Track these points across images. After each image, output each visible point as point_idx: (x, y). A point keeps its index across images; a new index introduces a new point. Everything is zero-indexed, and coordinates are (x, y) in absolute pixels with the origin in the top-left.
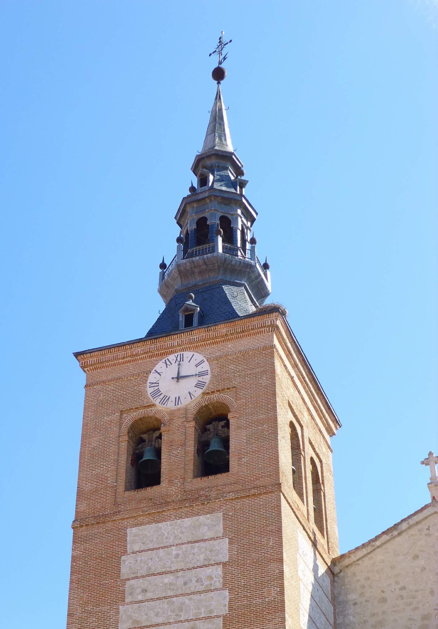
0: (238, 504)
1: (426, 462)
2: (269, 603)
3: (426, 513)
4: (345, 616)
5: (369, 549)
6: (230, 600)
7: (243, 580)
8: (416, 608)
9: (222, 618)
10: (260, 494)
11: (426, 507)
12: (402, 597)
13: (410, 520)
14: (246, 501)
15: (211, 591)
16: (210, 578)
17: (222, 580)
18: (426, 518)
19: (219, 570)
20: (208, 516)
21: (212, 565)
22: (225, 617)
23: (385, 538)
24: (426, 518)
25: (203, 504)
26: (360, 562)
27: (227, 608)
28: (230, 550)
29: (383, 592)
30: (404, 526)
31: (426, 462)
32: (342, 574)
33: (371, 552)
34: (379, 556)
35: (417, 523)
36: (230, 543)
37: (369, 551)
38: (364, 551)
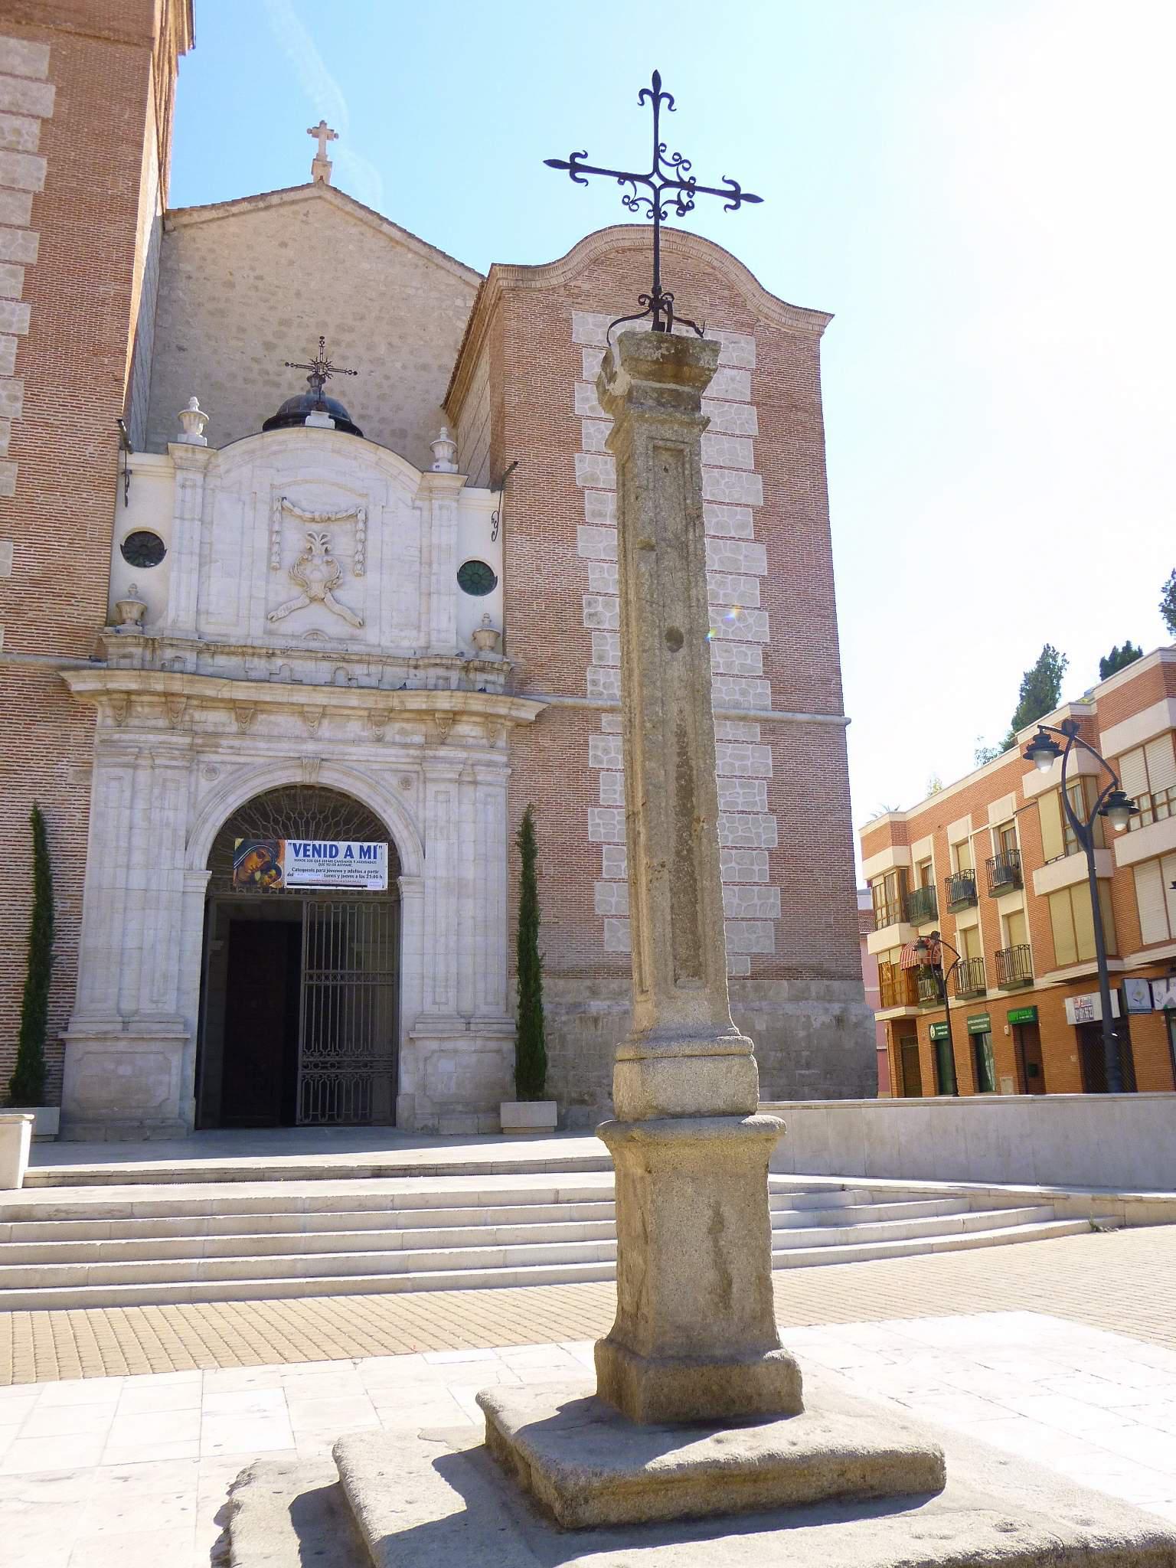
0: (80, 43)
1: (314, 132)
2: (113, 198)
3: (307, 193)
4: (171, 289)
5: (221, 213)
6: (49, 175)
7: (73, 154)
8: (271, 308)
9: (31, 196)
10: (118, 41)
11: (308, 185)
12: (256, 288)
13: (284, 195)
14: (93, 43)
15: (18, 151)
16: (18, 132)
17: (37, 142)
18: (306, 200)
19: (36, 127)
20: (25, 43)
21: (23, 115)
22: (37, 197)
23: (245, 206)
24: (306, 200)
25: (19, 22)
26: (204, 226)
27: (42, 183)
28: (57, 104)
29: (231, 274)
30: (275, 200)
31: (314, 132)
32: (175, 233)
33: (223, 218)
34: (232, 226)
35: (293, 202)
36: (60, 92)
37: (220, 216)
38: (214, 214)
